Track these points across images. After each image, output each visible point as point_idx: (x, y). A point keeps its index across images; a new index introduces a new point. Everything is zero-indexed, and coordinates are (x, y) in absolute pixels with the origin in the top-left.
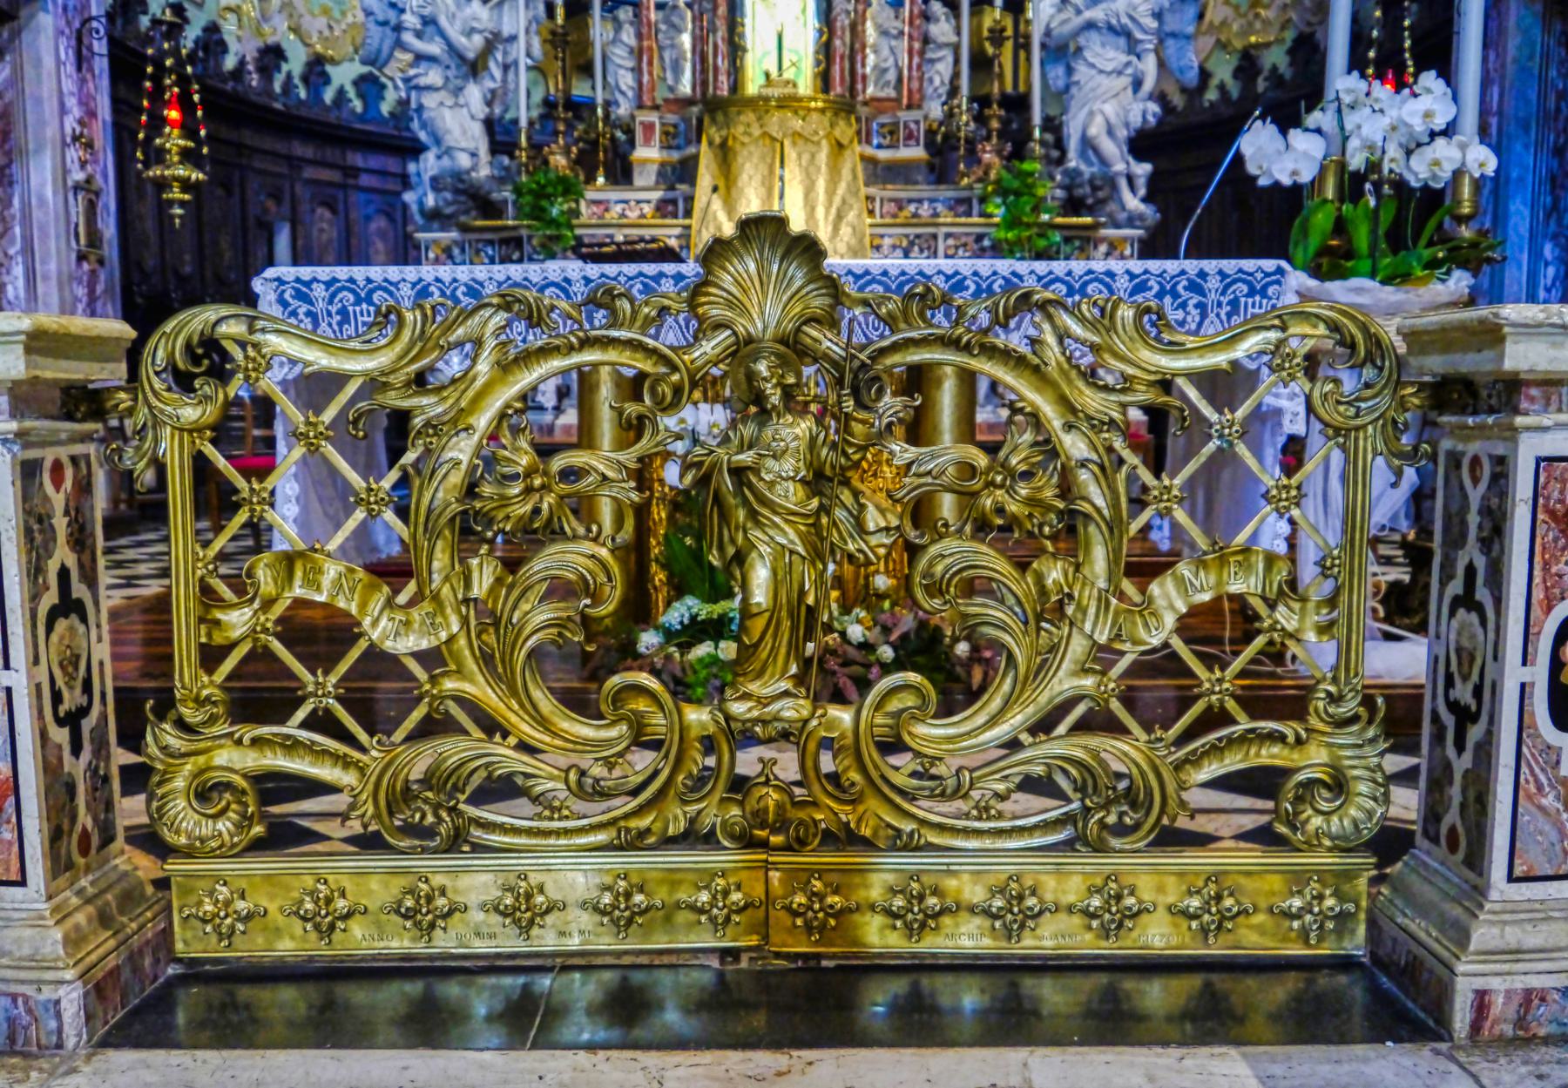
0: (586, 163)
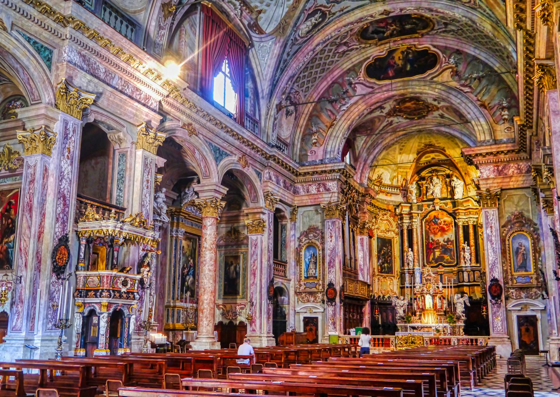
0: (412, 314)
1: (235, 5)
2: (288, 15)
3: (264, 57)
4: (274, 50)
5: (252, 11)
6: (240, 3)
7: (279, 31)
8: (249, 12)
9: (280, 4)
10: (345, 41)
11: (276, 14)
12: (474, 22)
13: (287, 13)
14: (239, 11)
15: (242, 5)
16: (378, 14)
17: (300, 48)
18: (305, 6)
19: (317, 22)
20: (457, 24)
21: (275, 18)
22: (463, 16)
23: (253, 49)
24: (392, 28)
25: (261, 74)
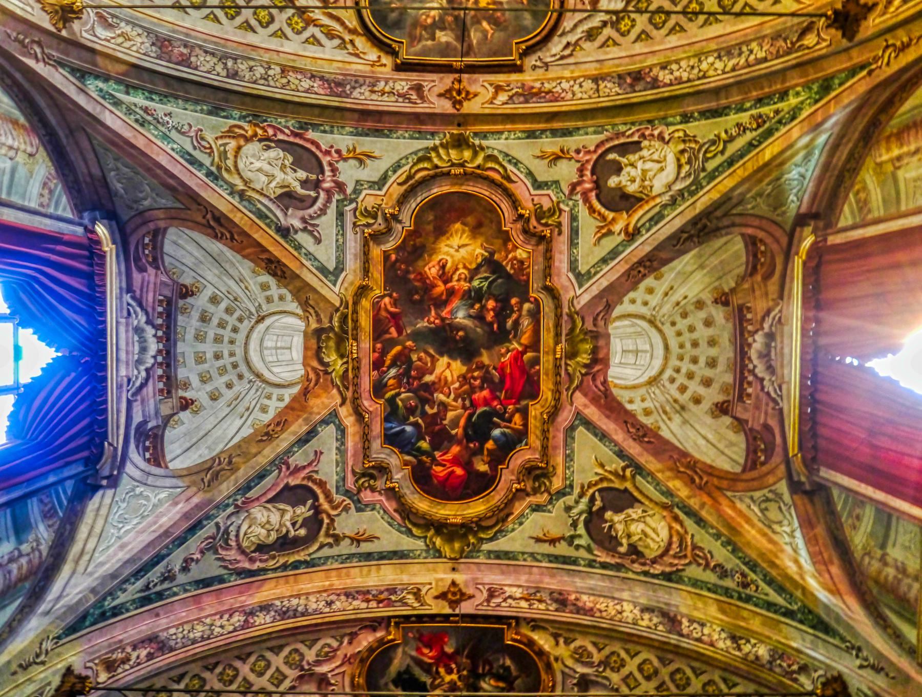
1: (143, 350)
2: (242, 450)
3: (124, 521)
4: (163, 514)
5: (169, 392)
6: (159, 352)
7: (203, 475)
8: (161, 391)
9: (241, 409)
10: (324, 669)
11: (217, 432)
12: (671, 620)
13: (244, 440)
14: (144, 374)
15: (160, 359)
16: (434, 592)
17: (220, 580)
18: (288, 452)
19: (292, 533)
20: (615, 678)
21: (210, 440)
22: (645, 609)
23: (110, 492)
24: (448, 678)
25: (86, 558)
